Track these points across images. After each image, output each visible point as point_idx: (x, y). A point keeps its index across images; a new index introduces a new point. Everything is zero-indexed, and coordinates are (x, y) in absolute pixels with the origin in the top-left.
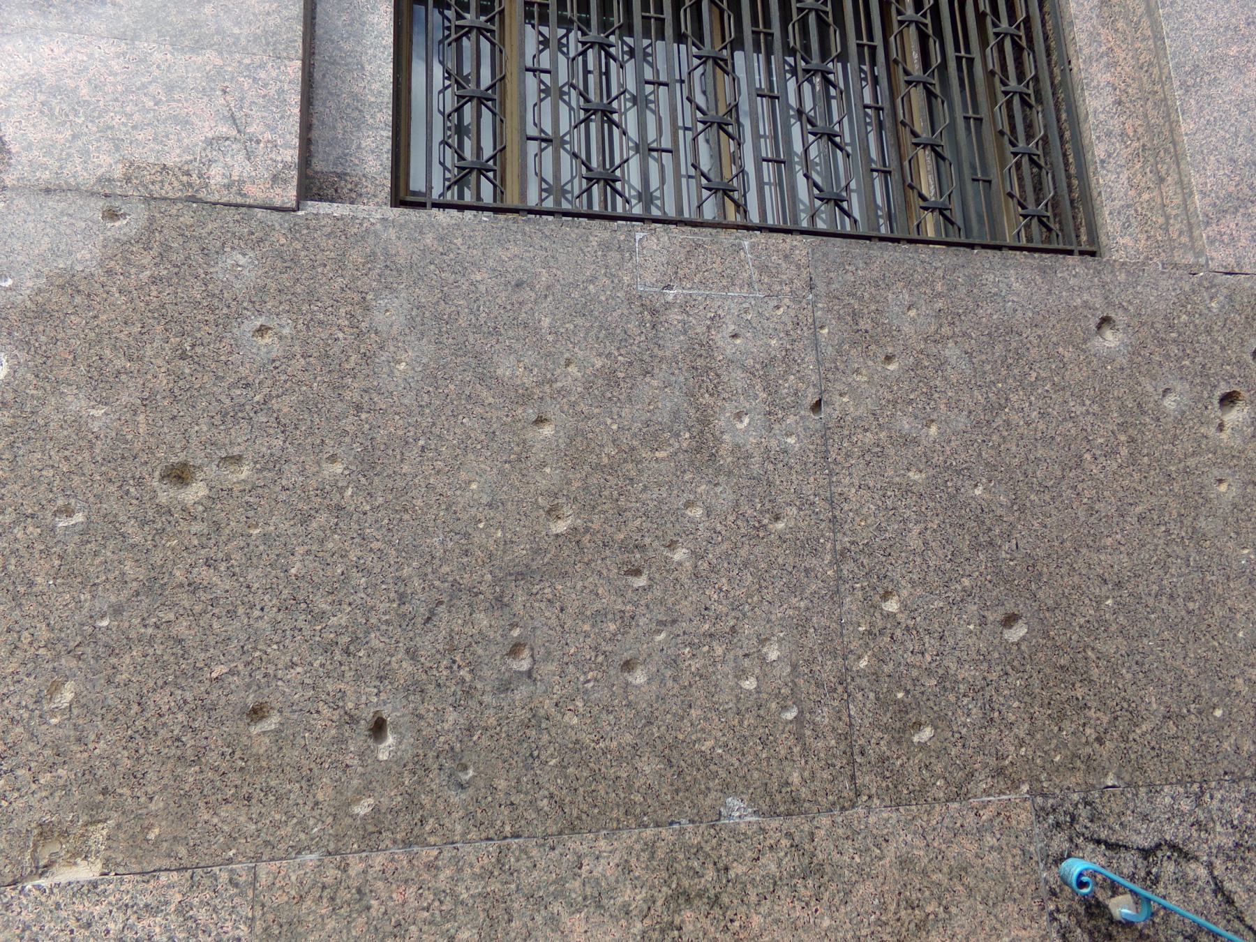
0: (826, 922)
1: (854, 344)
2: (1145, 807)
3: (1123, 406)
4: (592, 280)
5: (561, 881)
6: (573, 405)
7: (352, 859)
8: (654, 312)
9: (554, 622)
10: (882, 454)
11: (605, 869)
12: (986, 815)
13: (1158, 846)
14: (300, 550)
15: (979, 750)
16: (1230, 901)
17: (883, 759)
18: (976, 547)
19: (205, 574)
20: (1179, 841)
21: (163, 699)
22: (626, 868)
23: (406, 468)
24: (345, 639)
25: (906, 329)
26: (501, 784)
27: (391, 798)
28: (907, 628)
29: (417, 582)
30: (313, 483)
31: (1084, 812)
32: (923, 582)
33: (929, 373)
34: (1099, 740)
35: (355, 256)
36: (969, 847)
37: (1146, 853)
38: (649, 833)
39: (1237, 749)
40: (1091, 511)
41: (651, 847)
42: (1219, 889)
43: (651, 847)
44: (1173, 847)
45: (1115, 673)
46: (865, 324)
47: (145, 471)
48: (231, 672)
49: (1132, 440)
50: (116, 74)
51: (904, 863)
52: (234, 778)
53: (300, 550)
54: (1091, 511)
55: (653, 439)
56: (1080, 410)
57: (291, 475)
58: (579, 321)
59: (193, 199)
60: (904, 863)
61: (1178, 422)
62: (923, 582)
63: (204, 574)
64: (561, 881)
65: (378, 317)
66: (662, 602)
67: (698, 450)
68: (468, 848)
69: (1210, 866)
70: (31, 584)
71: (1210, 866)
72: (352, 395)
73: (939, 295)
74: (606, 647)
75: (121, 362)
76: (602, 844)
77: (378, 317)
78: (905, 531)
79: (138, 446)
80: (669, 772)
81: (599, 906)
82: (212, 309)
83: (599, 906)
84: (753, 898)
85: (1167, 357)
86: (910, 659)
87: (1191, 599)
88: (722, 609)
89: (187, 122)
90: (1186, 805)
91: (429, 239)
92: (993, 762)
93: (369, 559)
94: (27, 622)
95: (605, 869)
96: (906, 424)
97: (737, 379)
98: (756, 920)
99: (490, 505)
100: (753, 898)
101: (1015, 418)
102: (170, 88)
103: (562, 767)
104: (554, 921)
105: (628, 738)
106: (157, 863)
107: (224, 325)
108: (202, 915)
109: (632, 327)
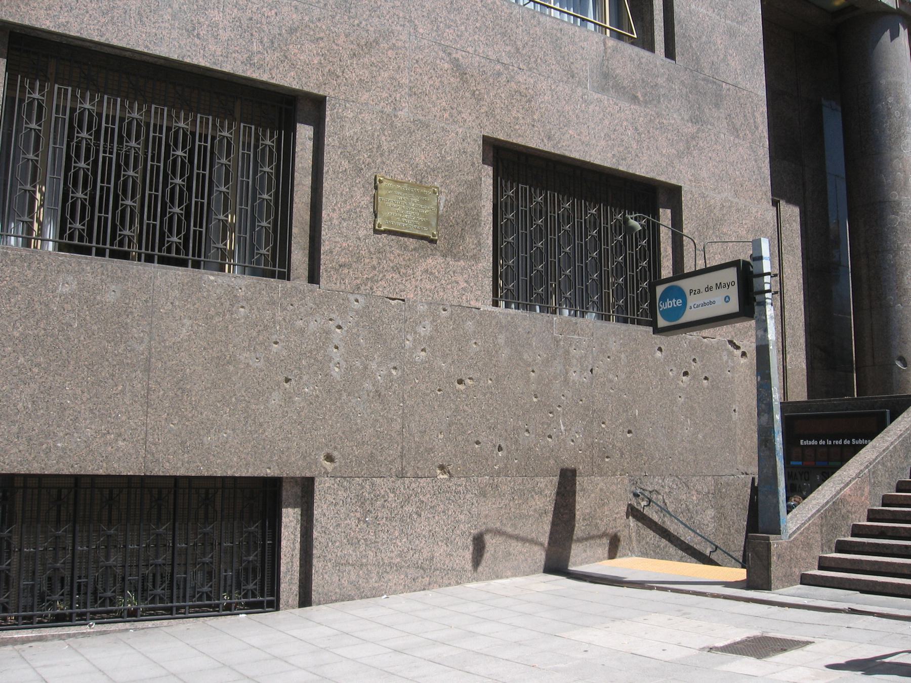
0: (585, 502)
1: (601, 353)
2: (652, 481)
3: (661, 374)
4: (544, 332)
5: (534, 487)
6: (539, 367)
7: (495, 478)
8: (557, 342)
9: (534, 424)
10: (605, 384)
11: (542, 485)
12: (619, 480)
13: (653, 491)
14: (484, 403)
15: (619, 464)
16: (666, 505)
17: (599, 465)
18: (624, 411)
19: (465, 407)
20: (658, 490)
21: (460, 438)
22: (546, 485)
23: (505, 383)
24: (493, 426)
25: (613, 348)
26: (523, 464)
27: (501, 465)
28: (607, 432)
29: (507, 412)
30: (486, 385)
31: (639, 481)
32: (611, 420)
33: (617, 361)
34: (645, 464)
35: (494, 323)
36: (614, 487)
37: (650, 492)
38: (551, 478)
39: (673, 468)
40: (650, 403)
41: (551, 481)
42: (664, 502)
43: (551, 481)
44: (656, 491)
45: (650, 448)
46: (604, 347)
47: (453, 381)
48: (472, 432)
49: (661, 384)
50: (442, 268)
51: (601, 490)
52: (473, 458)
53: (484, 403)
54: (650, 403)
55: (555, 378)
56: (650, 374)
57: (482, 384)
58: (541, 344)
59: (460, 306)
60: (601, 490)
61: (673, 379)
62: (611, 420)
63: (465, 407)
64: (534, 487)
65: (499, 340)
66: (556, 421)
67: (565, 381)
68: (516, 478)
69: (663, 496)
70: (434, 408)
71: (663, 496)
72: (494, 362)
73: (622, 339)
74: (545, 432)
75: (448, 352)
76: (542, 480)
77: (499, 340)
78: (608, 406)
79: (452, 374)
80: (555, 464)
81: (541, 494)
82: (465, 337)
83: (541, 494)
84: (571, 495)
85: (672, 360)
86: (607, 440)
87: (669, 429)
88: (568, 424)
89: (458, 283)
90: (660, 481)
91: (509, 319)
92: (621, 467)
93: (498, 406)
94: (434, 418)
95: (542, 485)
96: (611, 376)
97: (574, 361)
98: (571, 500)
99: (522, 393)
100: (571, 495)
101: (636, 376)
102: (454, 272)
103: (535, 460)
104: (532, 496)
105: (548, 454)
106: (461, 475)
107: (467, 341)
108: (469, 488)
109: (552, 346)
